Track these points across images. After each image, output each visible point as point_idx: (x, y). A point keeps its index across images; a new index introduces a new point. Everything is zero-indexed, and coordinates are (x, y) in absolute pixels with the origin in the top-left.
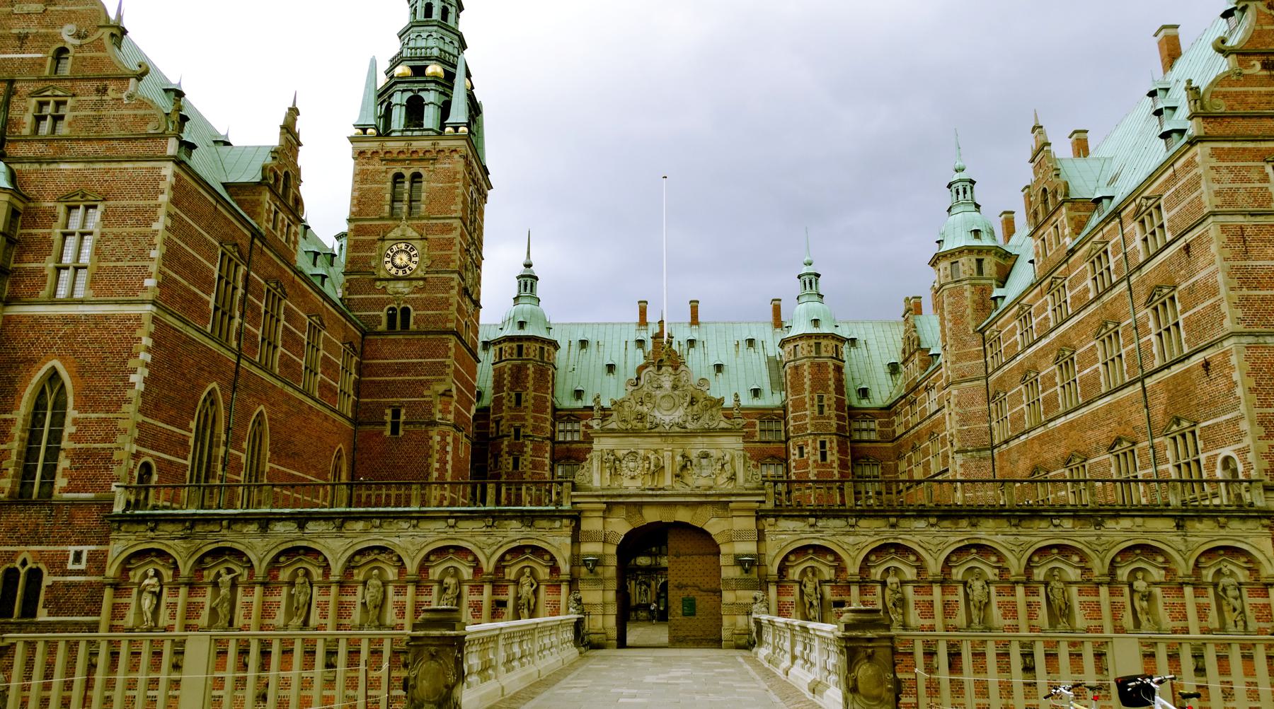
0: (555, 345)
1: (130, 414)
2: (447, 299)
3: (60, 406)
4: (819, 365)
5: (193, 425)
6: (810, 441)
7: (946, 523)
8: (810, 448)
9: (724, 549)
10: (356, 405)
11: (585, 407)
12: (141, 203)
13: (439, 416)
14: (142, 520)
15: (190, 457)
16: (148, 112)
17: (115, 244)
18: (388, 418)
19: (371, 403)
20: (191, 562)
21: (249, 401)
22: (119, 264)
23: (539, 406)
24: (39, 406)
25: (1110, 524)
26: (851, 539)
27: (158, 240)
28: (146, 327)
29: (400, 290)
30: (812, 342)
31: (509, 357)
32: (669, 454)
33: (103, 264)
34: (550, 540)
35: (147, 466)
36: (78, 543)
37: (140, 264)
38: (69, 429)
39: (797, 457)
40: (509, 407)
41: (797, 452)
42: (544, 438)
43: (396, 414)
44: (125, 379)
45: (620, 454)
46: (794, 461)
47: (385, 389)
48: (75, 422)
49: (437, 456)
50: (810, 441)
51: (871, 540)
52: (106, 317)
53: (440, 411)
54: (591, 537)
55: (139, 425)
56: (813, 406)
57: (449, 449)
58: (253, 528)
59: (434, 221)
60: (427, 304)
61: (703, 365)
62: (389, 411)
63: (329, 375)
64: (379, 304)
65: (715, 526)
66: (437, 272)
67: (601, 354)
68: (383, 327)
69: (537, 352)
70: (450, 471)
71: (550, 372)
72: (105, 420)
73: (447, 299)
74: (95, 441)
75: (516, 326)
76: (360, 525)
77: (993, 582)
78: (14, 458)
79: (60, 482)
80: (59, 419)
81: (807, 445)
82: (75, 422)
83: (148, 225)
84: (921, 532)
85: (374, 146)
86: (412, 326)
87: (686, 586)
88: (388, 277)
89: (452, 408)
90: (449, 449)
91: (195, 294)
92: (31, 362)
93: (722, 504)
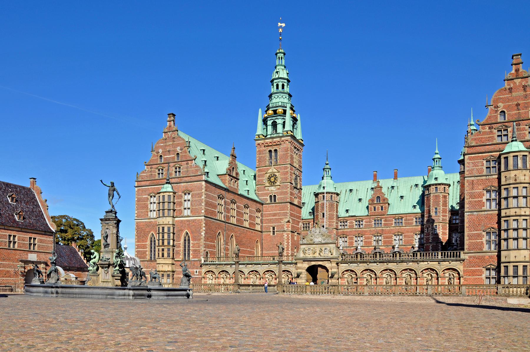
0: (338, 194)
1: (202, 242)
2: (287, 191)
3: (189, 240)
4: (436, 196)
5: (216, 242)
6: (431, 226)
7: (381, 264)
8: (430, 228)
9: (330, 270)
10: (261, 227)
11: (350, 216)
12: (199, 192)
13: (286, 229)
14: (207, 265)
15: (216, 249)
16: (199, 168)
17: (194, 202)
18: (272, 230)
19: (266, 225)
20: (218, 273)
21: (229, 233)
22: (196, 207)
23: (331, 218)
24: (185, 240)
25: (422, 263)
26: (357, 268)
27: (203, 201)
28: (203, 196)
29: (273, 190)
30: (434, 187)
31: (320, 200)
32: (317, 248)
33: (193, 207)
34: (290, 269)
35: (207, 252)
36: (196, 269)
37: (200, 207)
38: (191, 245)
39: (426, 232)
40: (320, 218)
41: (426, 230)
42: (333, 228)
43: (274, 228)
44: (200, 234)
45: (306, 249)
46: (426, 233)
47: (270, 221)
48: (192, 243)
49: (286, 241)
50: (431, 226)
51: (363, 268)
52: (195, 220)
53: (286, 227)
54: (300, 268)
55: (204, 244)
56: (433, 212)
57: (290, 238)
58: (229, 266)
59: (282, 166)
60: (281, 193)
61: (396, 197)
62: (272, 228)
63: (252, 220)
64: (266, 194)
65: (327, 264)
66: (283, 183)
67: (357, 194)
68: (269, 201)
69: (330, 198)
70: (290, 245)
71: (335, 204)
72: (198, 243)
73: (287, 191)
74: (196, 248)
75: (322, 188)
76: (250, 266)
77: (393, 277)
78: (182, 251)
79: (191, 256)
80: (189, 243)
81: (430, 227)
82: (192, 243)
83: (201, 197)
84: (375, 266)
85: (262, 141)
86: (277, 201)
87: (322, 279)
88: (269, 185)
89: (290, 226)
90: (290, 238)
91: (213, 210)
92: (182, 230)
93: (328, 260)
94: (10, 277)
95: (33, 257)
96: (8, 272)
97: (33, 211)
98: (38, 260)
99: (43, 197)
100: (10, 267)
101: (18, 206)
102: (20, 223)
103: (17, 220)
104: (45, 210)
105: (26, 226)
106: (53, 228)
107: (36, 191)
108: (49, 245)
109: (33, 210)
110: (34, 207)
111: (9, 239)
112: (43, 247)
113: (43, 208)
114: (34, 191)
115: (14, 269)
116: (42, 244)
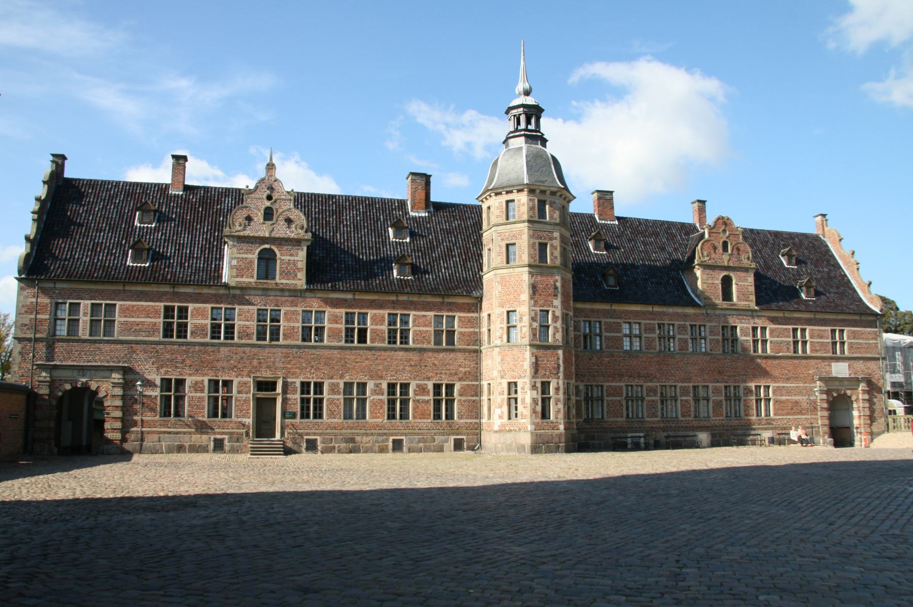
94: (800, 413)
95: (840, 370)
96: (797, 403)
97: (830, 277)
98: (853, 376)
99: (846, 247)
100: (800, 393)
101: (802, 271)
102: (811, 303)
103: (804, 298)
104: (852, 272)
105: (822, 307)
106: (876, 306)
107: (829, 238)
108: (872, 341)
109: (829, 274)
110: (830, 270)
111: (795, 336)
112: (859, 347)
113: (847, 269)
114: (825, 240)
115: (807, 397)
116: (857, 341)
